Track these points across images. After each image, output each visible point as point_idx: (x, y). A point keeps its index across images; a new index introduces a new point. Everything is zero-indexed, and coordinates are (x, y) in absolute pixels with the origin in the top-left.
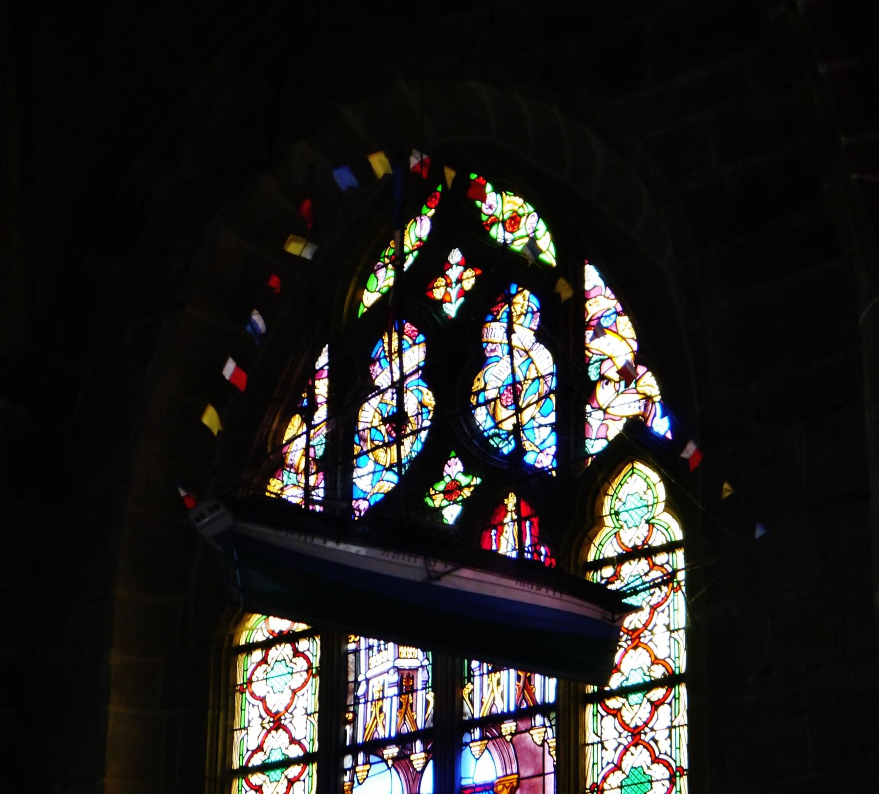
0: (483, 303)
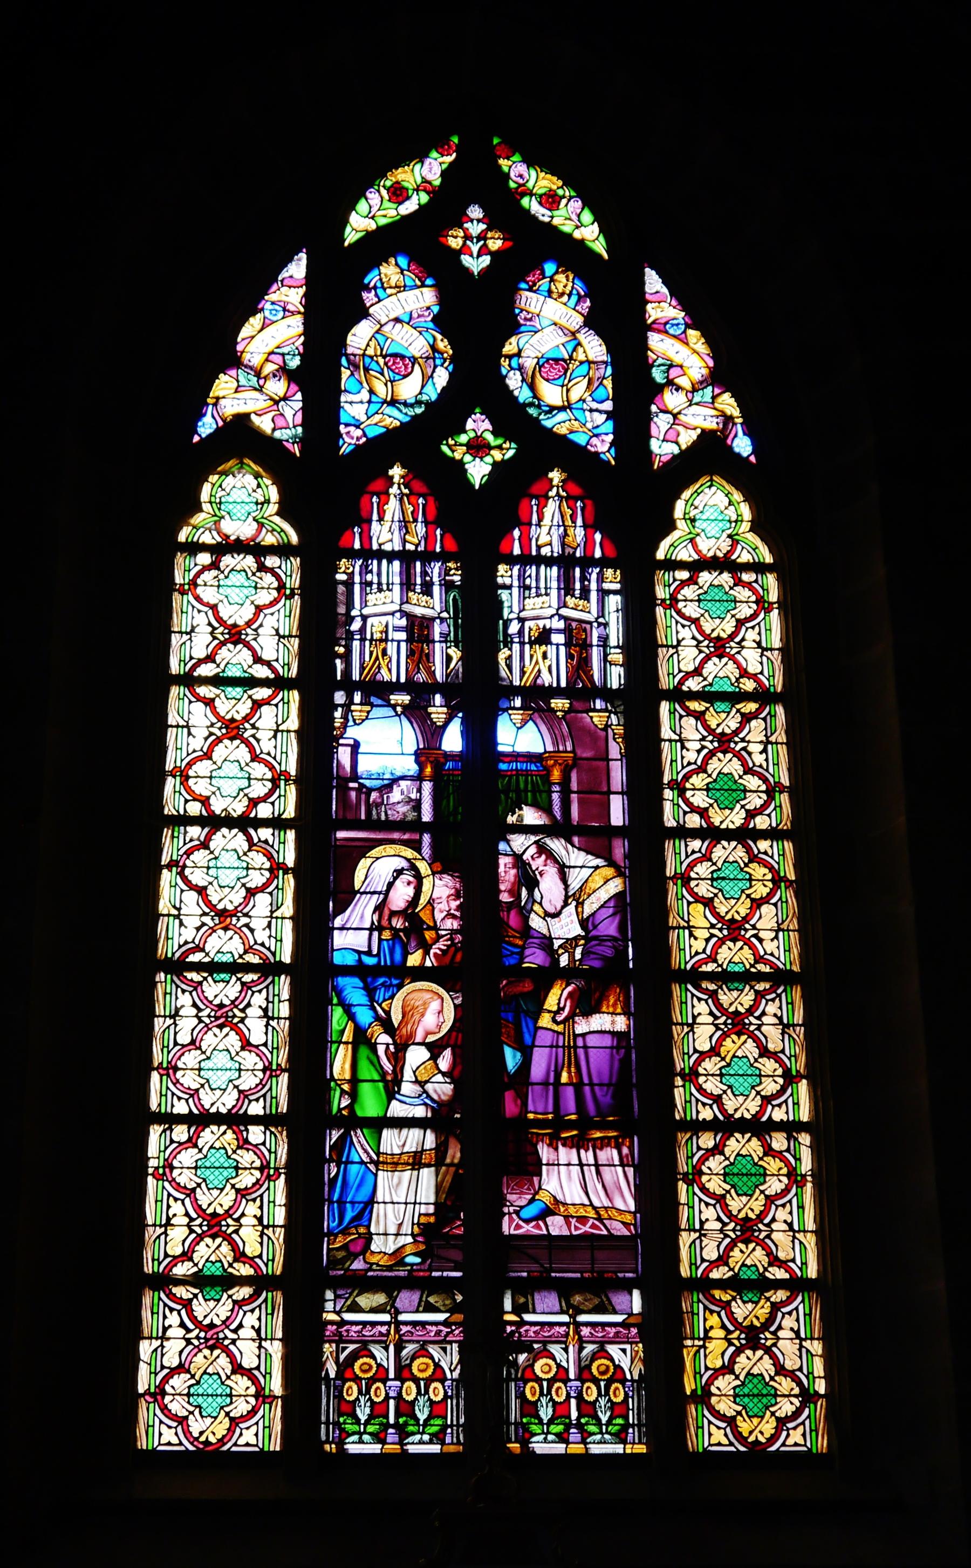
0: (513, 270)
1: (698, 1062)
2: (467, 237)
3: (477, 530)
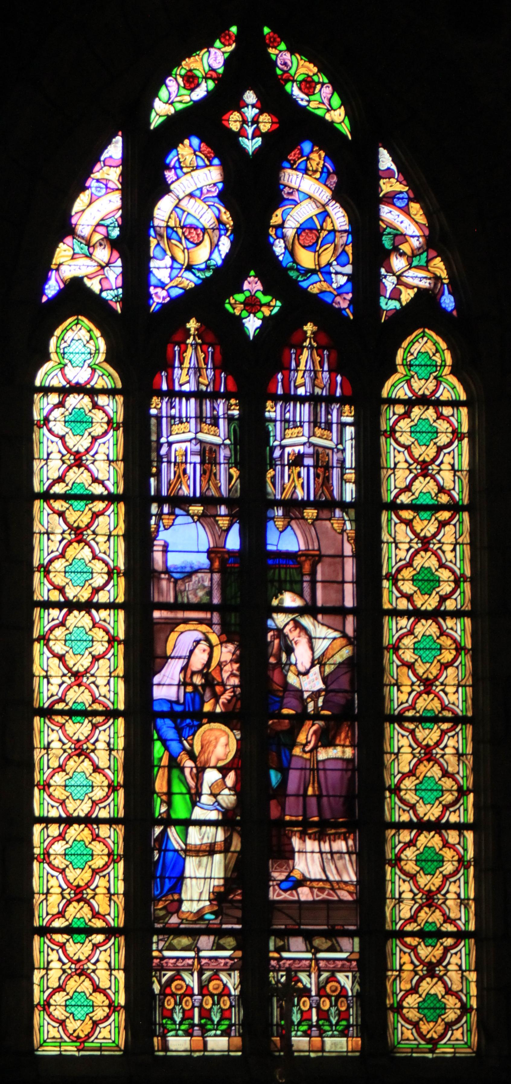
0: (278, 149)
1: (401, 781)
2: (244, 121)
3: (250, 373)
